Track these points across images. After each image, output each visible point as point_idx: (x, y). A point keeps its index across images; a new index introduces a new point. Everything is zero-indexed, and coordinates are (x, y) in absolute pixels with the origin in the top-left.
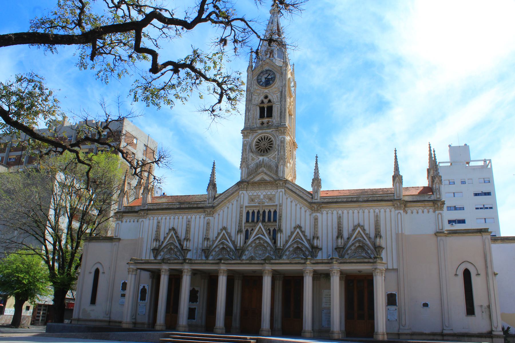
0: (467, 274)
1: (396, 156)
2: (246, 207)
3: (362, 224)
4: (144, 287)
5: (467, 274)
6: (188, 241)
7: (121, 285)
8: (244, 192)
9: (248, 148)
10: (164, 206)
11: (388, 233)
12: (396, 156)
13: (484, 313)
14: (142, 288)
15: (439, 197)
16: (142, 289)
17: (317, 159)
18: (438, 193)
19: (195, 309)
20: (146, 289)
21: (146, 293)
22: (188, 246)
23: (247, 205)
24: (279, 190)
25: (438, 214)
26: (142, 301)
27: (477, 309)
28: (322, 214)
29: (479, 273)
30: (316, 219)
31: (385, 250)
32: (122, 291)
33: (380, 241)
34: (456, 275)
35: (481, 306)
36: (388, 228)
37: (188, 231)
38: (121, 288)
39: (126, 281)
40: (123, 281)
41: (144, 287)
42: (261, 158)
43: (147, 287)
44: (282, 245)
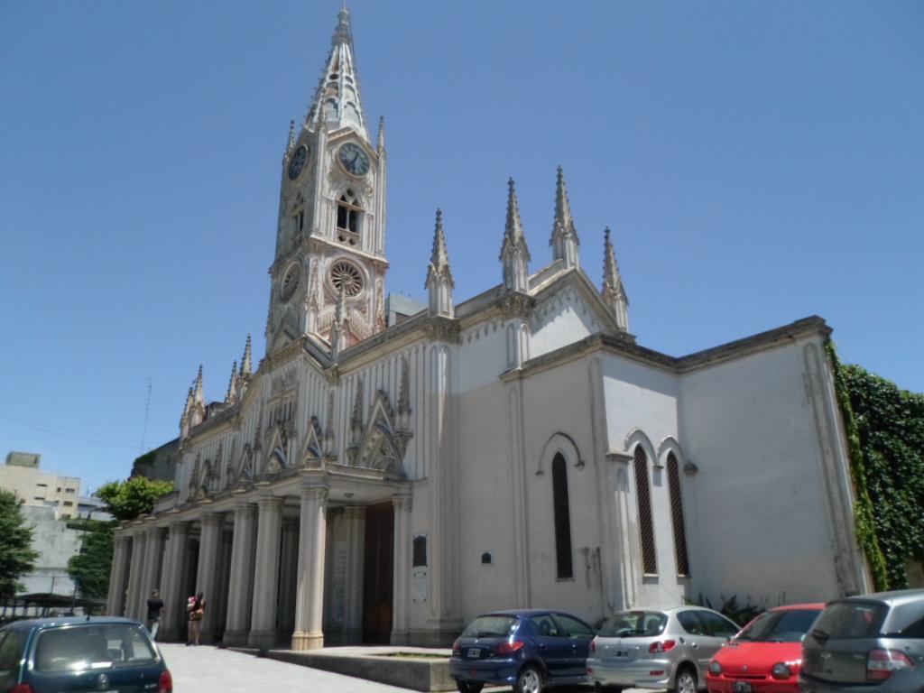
0: (559, 464)
2: (269, 402)
3: (386, 390)
5: (559, 464)
6: (216, 479)
8: (267, 375)
9: (276, 295)
11: (420, 397)
13: (591, 570)
15: (509, 287)
18: (509, 278)
22: (215, 487)
23: (269, 396)
24: (298, 357)
25: (508, 329)
27: (578, 562)
28: (341, 385)
29: (583, 458)
30: (332, 397)
31: (414, 439)
33: (401, 421)
34: (539, 473)
35: (586, 551)
36: (420, 390)
37: (218, 461)
42: (286, 307)
44: (293, 462)
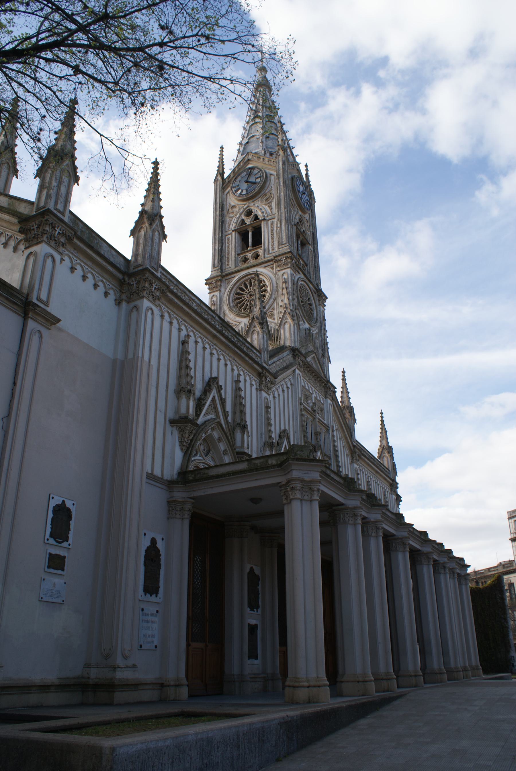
1: (382, 421)
4: (153, 541)
7: (51, 515)
10: (194, 304)
12: (382, 421)
14: (148, 544)
16: (148, 551)
17: (344, 376)
19: (256, 625)
20: (158, 550)
21: (159, 566)
26: (148, 595)
32: (52, 541)
38: (49, 530)
39: (69, 504)
40: (57, 501)
41: (153, 541)
43: (160, 545)
